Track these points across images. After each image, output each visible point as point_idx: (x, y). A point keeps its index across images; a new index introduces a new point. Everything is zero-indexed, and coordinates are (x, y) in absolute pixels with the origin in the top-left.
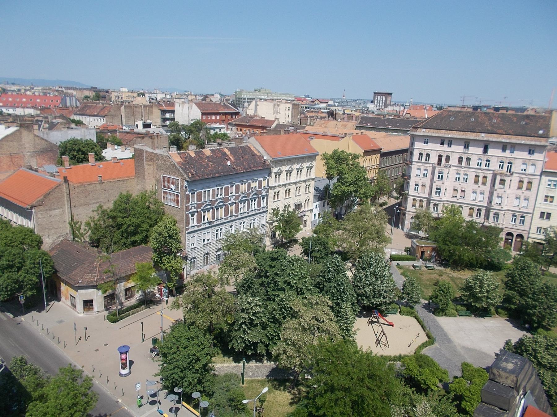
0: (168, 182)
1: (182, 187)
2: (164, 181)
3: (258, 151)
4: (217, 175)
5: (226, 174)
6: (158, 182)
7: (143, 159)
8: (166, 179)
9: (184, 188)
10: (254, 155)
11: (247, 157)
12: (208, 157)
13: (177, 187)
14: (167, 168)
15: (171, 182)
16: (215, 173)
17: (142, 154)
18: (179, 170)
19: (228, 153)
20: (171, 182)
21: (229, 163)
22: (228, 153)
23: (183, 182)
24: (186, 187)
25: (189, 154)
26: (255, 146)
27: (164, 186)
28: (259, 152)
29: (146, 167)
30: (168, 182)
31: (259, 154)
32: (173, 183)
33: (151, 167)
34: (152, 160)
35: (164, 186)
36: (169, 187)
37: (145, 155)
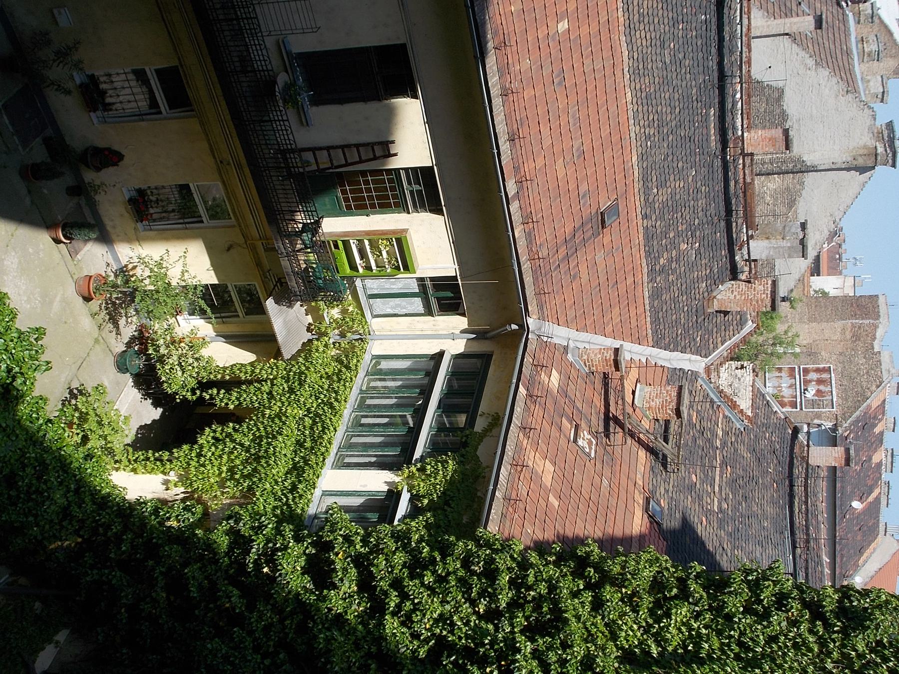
0: (820, 382)
1: (818, 416)
2: (818, 370)
3: (868, 558)
4: (838, 485)
5: (838, 503)
6: (811, 353)
7: (854, 316)
8: (825, 376)
9: (816, 421)
10: (861, 551)
11: (859, 538)
12: (870, 459)
13: (813, 404)
14: (852, 379)
15: (822, 388)
16: (842, 482)
17: (866, 316)
18: (856, 408)
19: (871, 498)
20: (822, 388)
21: (856, 504)
22: (871, 498)
23: (828, 419)
24: (819, 426)
25: (880, 420)
26: (878, 551)
27: (806, 371)
28: (866, 562)
29: (839, 324)
30: (820, 382)
31: (861, 562)
32: (819, 393)
33: (837, 336)
34: (856, 337)
35: (806, 371)
36: (807, 382)
37: (867, 322)
